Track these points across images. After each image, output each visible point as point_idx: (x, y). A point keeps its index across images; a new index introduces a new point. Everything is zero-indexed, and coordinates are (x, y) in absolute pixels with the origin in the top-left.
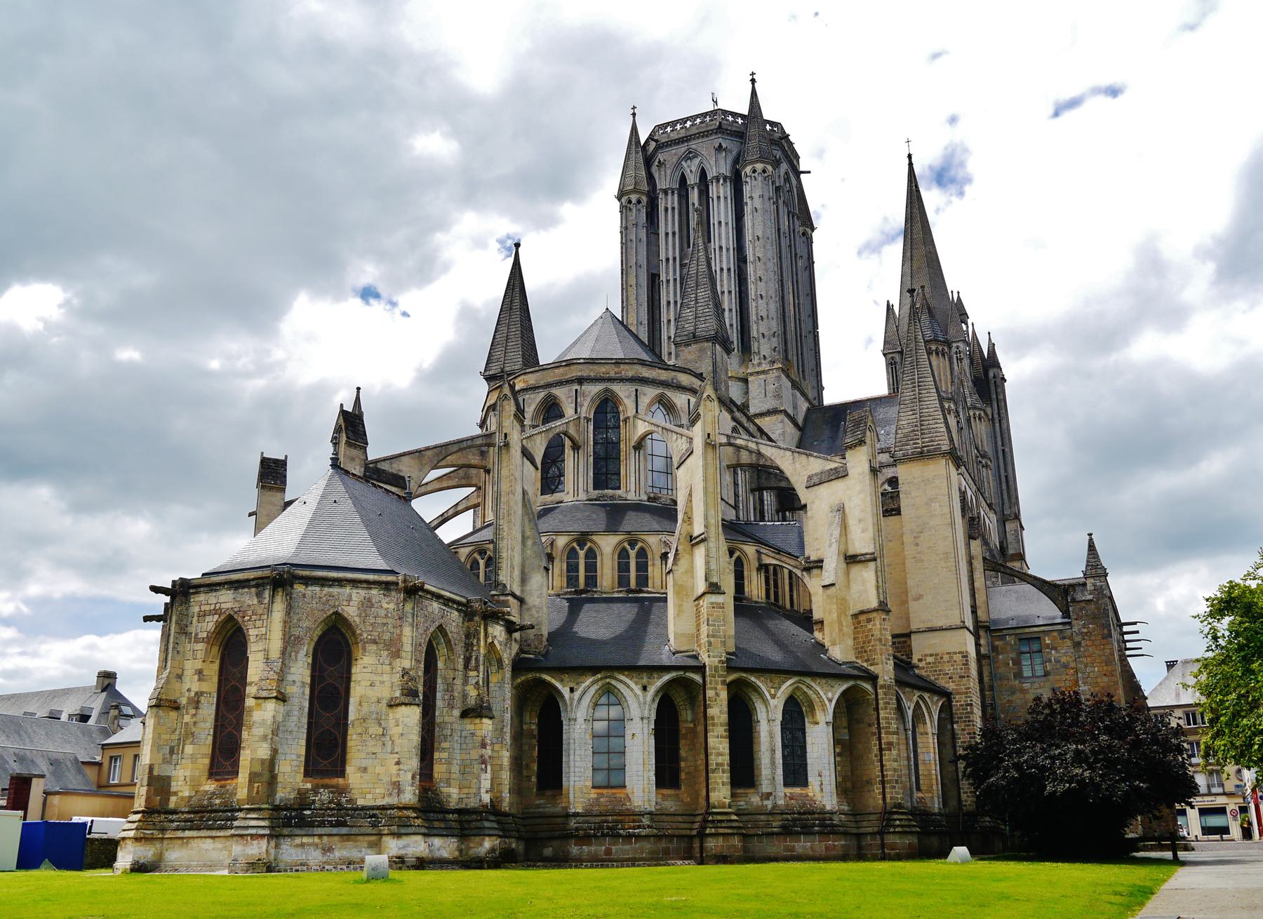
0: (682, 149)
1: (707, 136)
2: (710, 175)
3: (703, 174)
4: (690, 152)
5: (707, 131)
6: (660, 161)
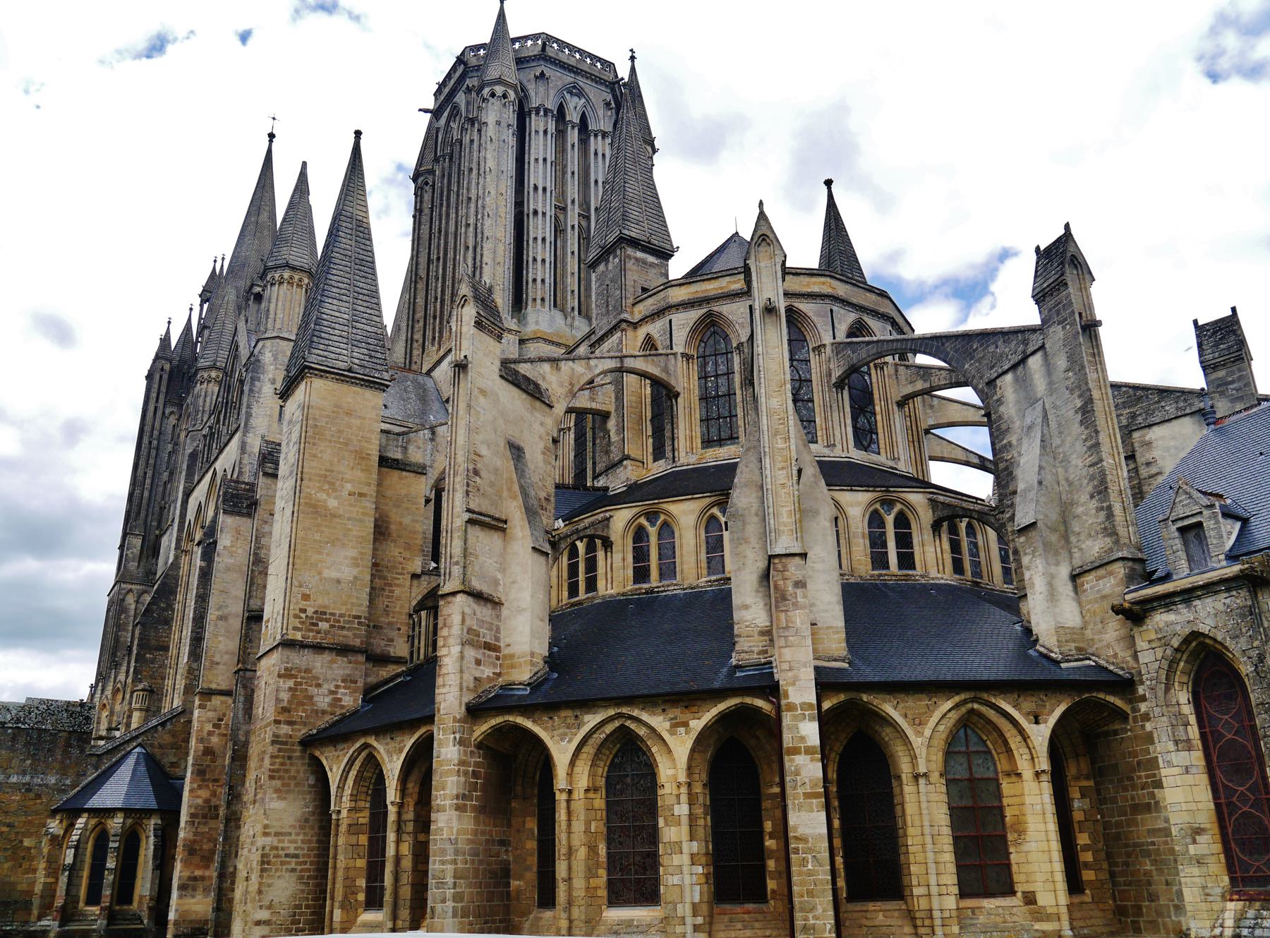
0: (569, 78)
1: (596, 82)
2: (592, 126)
3: (583, 118)
4: (574, 87)
5: (601, 79)
6: (542, 74)
